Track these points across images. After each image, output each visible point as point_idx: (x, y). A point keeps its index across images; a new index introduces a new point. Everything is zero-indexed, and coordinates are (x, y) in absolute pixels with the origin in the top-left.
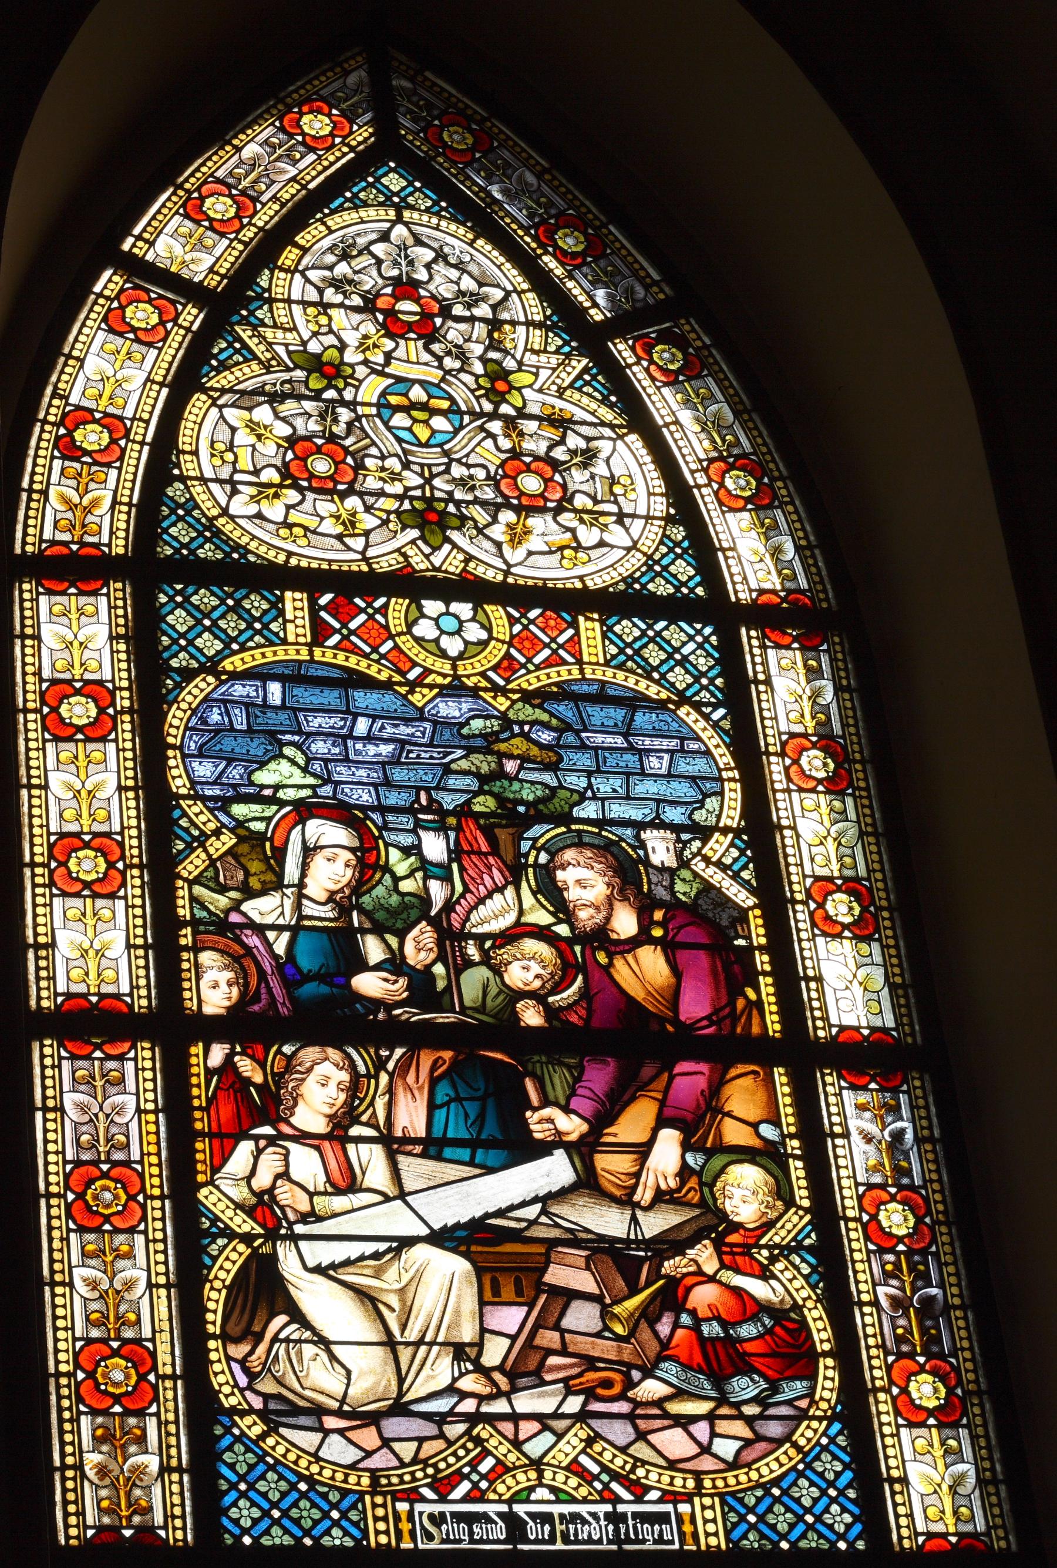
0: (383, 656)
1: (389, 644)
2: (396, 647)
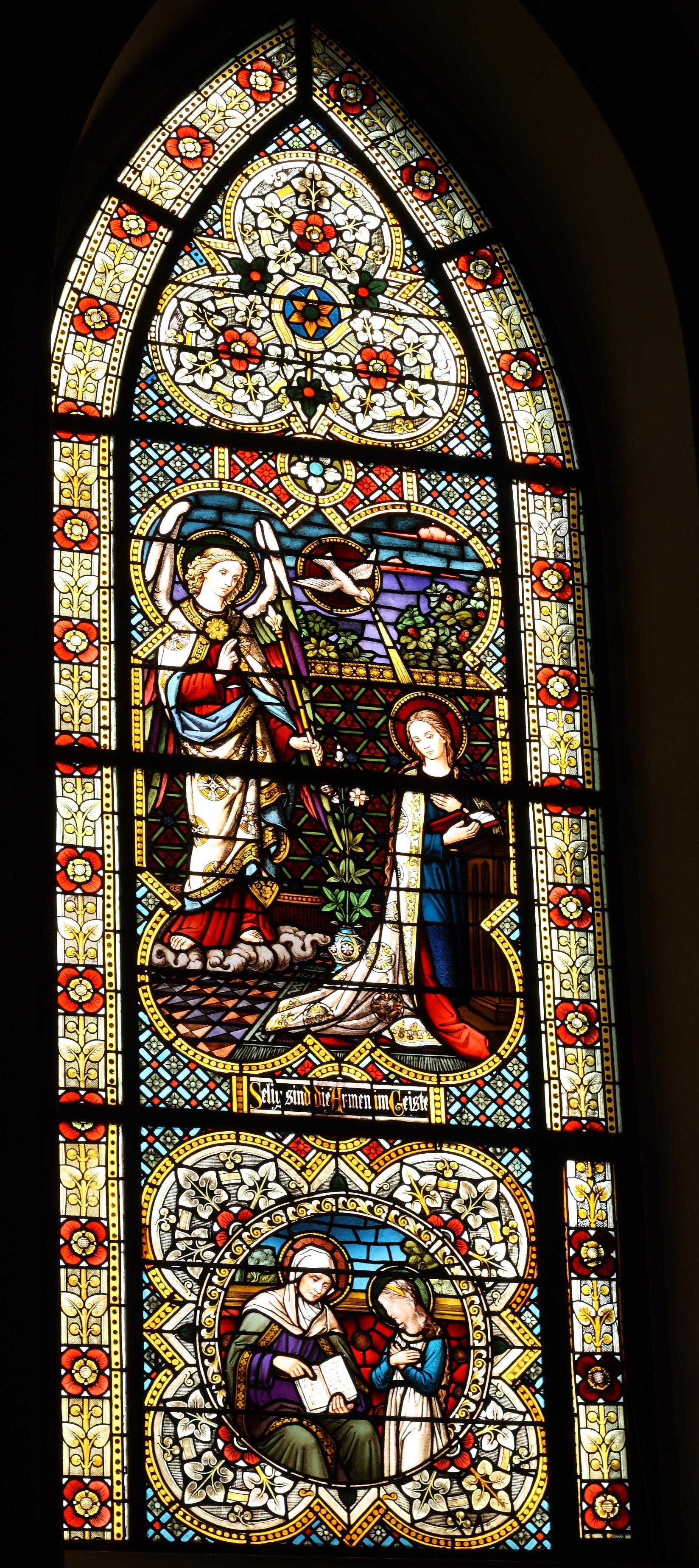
0: (271, 490)
1: (276, 481)
2: (280, 483)
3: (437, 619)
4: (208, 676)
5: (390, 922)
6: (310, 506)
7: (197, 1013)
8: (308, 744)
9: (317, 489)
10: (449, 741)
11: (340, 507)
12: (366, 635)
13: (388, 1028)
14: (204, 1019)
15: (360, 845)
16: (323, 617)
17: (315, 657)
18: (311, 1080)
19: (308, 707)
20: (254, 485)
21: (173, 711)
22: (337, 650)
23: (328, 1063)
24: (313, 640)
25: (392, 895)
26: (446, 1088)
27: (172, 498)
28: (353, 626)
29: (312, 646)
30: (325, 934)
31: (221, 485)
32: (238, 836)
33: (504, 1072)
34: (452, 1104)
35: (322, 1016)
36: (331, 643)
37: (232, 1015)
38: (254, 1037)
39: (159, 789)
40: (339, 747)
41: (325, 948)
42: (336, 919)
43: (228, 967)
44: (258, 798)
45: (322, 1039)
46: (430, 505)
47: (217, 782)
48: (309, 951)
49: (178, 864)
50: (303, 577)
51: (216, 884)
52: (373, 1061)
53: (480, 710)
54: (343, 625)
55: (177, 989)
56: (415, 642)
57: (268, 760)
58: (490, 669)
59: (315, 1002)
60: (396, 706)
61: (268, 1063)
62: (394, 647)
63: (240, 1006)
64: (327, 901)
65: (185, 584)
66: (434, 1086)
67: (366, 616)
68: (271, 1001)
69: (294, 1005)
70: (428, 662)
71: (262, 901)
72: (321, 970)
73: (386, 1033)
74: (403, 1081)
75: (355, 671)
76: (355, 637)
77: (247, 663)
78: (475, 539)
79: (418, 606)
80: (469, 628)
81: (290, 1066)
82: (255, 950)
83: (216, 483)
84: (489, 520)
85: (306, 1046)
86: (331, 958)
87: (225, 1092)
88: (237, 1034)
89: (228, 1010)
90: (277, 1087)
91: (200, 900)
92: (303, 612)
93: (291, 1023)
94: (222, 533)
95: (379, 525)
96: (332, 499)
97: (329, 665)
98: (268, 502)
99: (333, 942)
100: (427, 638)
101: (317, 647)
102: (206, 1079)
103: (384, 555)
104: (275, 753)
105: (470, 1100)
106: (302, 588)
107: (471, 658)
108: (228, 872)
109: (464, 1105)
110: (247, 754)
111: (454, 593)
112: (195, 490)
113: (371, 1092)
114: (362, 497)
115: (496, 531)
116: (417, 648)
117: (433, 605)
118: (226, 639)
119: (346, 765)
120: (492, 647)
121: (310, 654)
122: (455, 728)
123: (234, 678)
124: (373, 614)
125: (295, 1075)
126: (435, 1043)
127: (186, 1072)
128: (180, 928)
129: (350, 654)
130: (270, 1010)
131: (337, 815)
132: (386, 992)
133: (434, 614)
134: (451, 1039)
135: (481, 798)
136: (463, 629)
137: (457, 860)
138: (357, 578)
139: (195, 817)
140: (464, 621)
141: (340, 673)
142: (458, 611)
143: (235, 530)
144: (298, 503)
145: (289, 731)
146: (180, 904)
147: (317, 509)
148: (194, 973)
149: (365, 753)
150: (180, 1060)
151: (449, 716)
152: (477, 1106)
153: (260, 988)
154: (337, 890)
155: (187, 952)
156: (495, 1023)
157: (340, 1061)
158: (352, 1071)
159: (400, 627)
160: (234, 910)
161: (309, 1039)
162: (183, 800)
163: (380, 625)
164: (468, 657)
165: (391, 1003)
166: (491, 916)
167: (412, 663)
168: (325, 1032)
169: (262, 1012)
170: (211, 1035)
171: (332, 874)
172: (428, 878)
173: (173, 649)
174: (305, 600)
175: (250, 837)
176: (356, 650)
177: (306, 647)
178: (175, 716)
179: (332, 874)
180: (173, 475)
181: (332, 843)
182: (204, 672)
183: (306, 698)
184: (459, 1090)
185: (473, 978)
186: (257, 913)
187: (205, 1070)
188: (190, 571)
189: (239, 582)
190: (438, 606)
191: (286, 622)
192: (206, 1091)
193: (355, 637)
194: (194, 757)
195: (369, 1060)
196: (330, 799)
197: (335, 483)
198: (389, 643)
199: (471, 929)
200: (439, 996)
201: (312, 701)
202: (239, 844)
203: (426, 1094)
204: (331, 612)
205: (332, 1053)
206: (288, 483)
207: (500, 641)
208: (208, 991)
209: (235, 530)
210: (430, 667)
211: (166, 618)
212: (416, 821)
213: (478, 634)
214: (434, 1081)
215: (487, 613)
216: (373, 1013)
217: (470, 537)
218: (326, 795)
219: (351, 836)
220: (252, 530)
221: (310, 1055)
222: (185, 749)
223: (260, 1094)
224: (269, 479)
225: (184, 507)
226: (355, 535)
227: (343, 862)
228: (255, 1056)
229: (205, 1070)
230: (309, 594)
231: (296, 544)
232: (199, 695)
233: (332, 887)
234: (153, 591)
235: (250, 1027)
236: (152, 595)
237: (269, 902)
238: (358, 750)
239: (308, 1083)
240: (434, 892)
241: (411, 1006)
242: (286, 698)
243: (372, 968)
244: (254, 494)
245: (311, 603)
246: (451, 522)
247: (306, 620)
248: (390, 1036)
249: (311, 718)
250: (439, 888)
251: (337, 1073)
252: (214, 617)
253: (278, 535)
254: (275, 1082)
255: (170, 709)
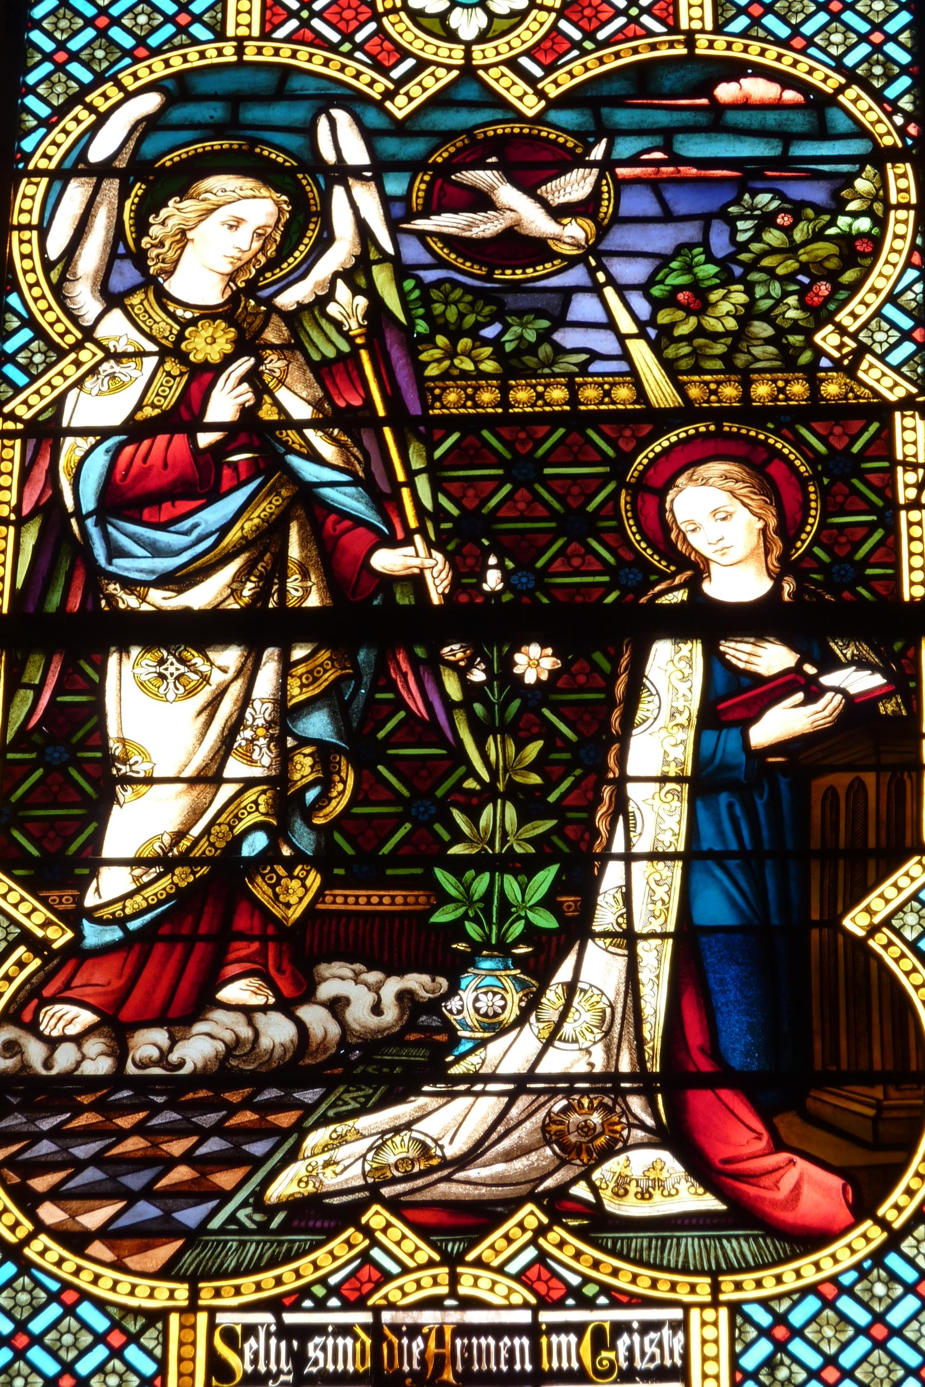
1: (372, 27)
2: (381, 30)
3: (752, 266)
4: (180, 440)
5: (605, 935)
6: (449, 68)
7: (91, 1174)
8: (416, 562)
9: (468, 32)
10: (773, 522)
11: (525, 61)
12: (572, 316)
13: (585, 1176)
14: (110, 1186)
15: (533, 767)
16: (467, 289)
17: (445, 376)
18: (377, 1311)
19: (422, 483)
20: (320, 42)
21: (90, 522)
22: (499, 354)
23: (420, 1268)
24: (441, 340)
25: (614, 873)
26: (735, 1308)
27: (121, 87)
28: (540, 301)
29: (437, 353)
30: (434, 973)
31: (240, 51)
32: (227, 774)
33: (892, 1260)
34: (748, 1346)
35: (413, 1161)
36: (485, 342)
37: (182, 1173)
38: (232, 1219)
39: (38, 690)
40: (492, 561)
41: (434, 1006)
42: (466, 938)
43: (182, 1064)
44: (283, 687)
45: (411, 1214)
46: (744, 34)
47: (182, 661)
48: (391, 1014)
49: (73, 848)
50: (425, 214)
51: (165, 882)
52: (543, 1256)
53: (856, 449)
54: (512, 301)
55: (46, 1125)
56: (693, 321)
57: (314, 601)
58: (882, 358)
59: (397, 1130)
60: (642, 459)
61: (267, 1277)
62: (642, 335)
63: (202, 1150)
64: (445, 899)
65: (139, 258)
66: (702, 1306)
67: (576, 276)
68: (283, 1134)
69: (342, 1140)
70: (726, 358)
71: (277, 911)
72: (420, 1056)
73: (581, 1190)
74: (618, 1299)
75: (540, 396)
76: (545, 324)
77: (276, 403)
78: (854, 91)
79: (705, 244)
80: (832, 277)
81: (323, 1281)
82: (251, 1023)
83: (229, 48)
84: (891, 48)
85: (367, 1231)
86: (448, 1028)
87: (149, 1353)
88: (190, 1216)
89: (171, 1163)
90: (285, 1332)
91: (121, 922)
92: (420, 283)
93: (331, 1180)
94: (235, 144)
95: (616, 88)
96: (504, 48)
97: (477, 389)
98: (350, 71)
99: (454, 989)
100: (725, 307)
101: (451, 354)
102: (100, 1323)
103: (625, 148)
104: (332, 585)
105: (797, 1333)
106: (422, 235)
107: (835, 339)
108: (196, 853)
109: (780, 1346)
110: (261, 595)
111: (797, 209)
112: (177, 64)
113: (533, 1331)
114: (577, 35)
115: (905, 70)
116: (700, 331)
117: (741, 237)
118: (228, 360)
119: (507, 598)
120: (890, 311)
121: (432, 371)
122: (790, 495)
123: (243, 439)
124: (592, 272)
125: (334, 1302)
126: (710, 1203)
127: (55, 1310)
128: (67, 986)
129: (530, 361)
130: (278, 1156)
131: (478, 708)
132: (584, 1092)
133: (744, 257)
134: (752, 1191)
135: (849, 636)
136: (815, 280)
137: (784, 783)
138: (557, 200)
139: (123, 741)
140: (820, 263)
141: (504, 402)
142: (805, 244)
143: (267, 135)
144: (422, 64)
145: (372, 537)
146: (70, 935)
147: (468, 71)
148: (93, 1083)
149: (557, 566)
150: (38, 1284)
151: (775, 469)
152: (815, 1347)
153: (254, 1108)
154: (470, 874)
155: (78, 1040)
156: (875, 1145)
157: (452, 1261)
158: (485, 1283)
159: (656, 291)
160: (205, 938)
161: (376, 1217)
162: (98, 708)
163: (609, 292)
164: (827, 339)
165: (596, 1118)
166: (873, 900)
167: (684, 364)
168: (418, 1197)
169: (256, 1163)
170: (123, 1222)
171: (458, 837)
172: (706, 829)
173: (100, 393)
174: (427, 258)
175: (258, 772)
176: (545, 350)
177: (424, 357)
178: (94, 532)
179: (458, 837)
180: (128, 42)
181: (462, 770)
182: (172, 432)
183: (417, 463)
184: (770, 1310)
185: (818, 1046)
186: (264, 939)
187: (101, 1304)
188: (154, 231)
189: (268, 239)
190: (757, 238)
191: (377, 307)
192: (101, 1352)
193: (545, 324)
194: (133, 614)
195: (531, 1253)
196: (462, 673)
197: (513, 14)
198: (626, 325)
199: (815, 933)
200: (727, 1095)
201: (433, 469)
202: (227, 791)
203: (682, 1326)
204: (488, 278)
205: (433, 1245)
206: (400, 27)
207: (910, 295)
208: (125, 1122)
209: (267, 135)
210: (730, 368)
211: (88, 333)
212: (680, 705)
213: (854, 288)
214: (704, 1294)
215: (877, 242)
216: (548, 1143)
217: (841, 89)
218: (453, 666)
219: (511, 749)
220: (310, 131)
221: (376, 1253)
222: (111, 598)
223: (241, 1354)
224: (354, 24)
225: (150, 102)
226: (555, 116)
227: (488, 810)
228: (231, 1263)
229: (101, 1304)
230: (437, 247)
231: (413, 148)
232: (153, 483)
233: (457, 866)
234: (63, 279)
235: (225, 1196)
236: (58, 291)
237: (295, 913)
238: (540, 564)
239: (366, 1317)
240: (719, 857)
241: (650, 1122)
242: (367, 469)
243: (548, 1043)
244: (318, 60)
245: (441, 263)
246: (795, 63)
247: (426, 301)
248: (590, 1197)
249: (428, 504)
250: (734, 846)
251: (444, 1290)
252: (202, 317)
253: (369, 135)
254: (279, 1322)
255: (81, 519)
